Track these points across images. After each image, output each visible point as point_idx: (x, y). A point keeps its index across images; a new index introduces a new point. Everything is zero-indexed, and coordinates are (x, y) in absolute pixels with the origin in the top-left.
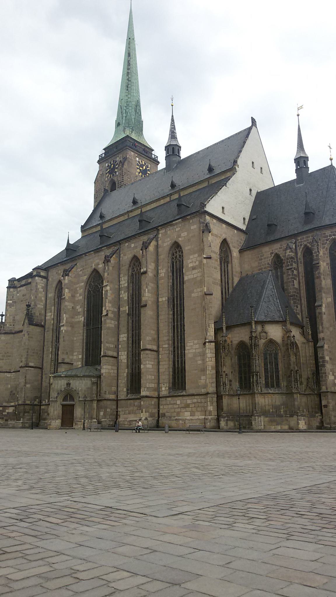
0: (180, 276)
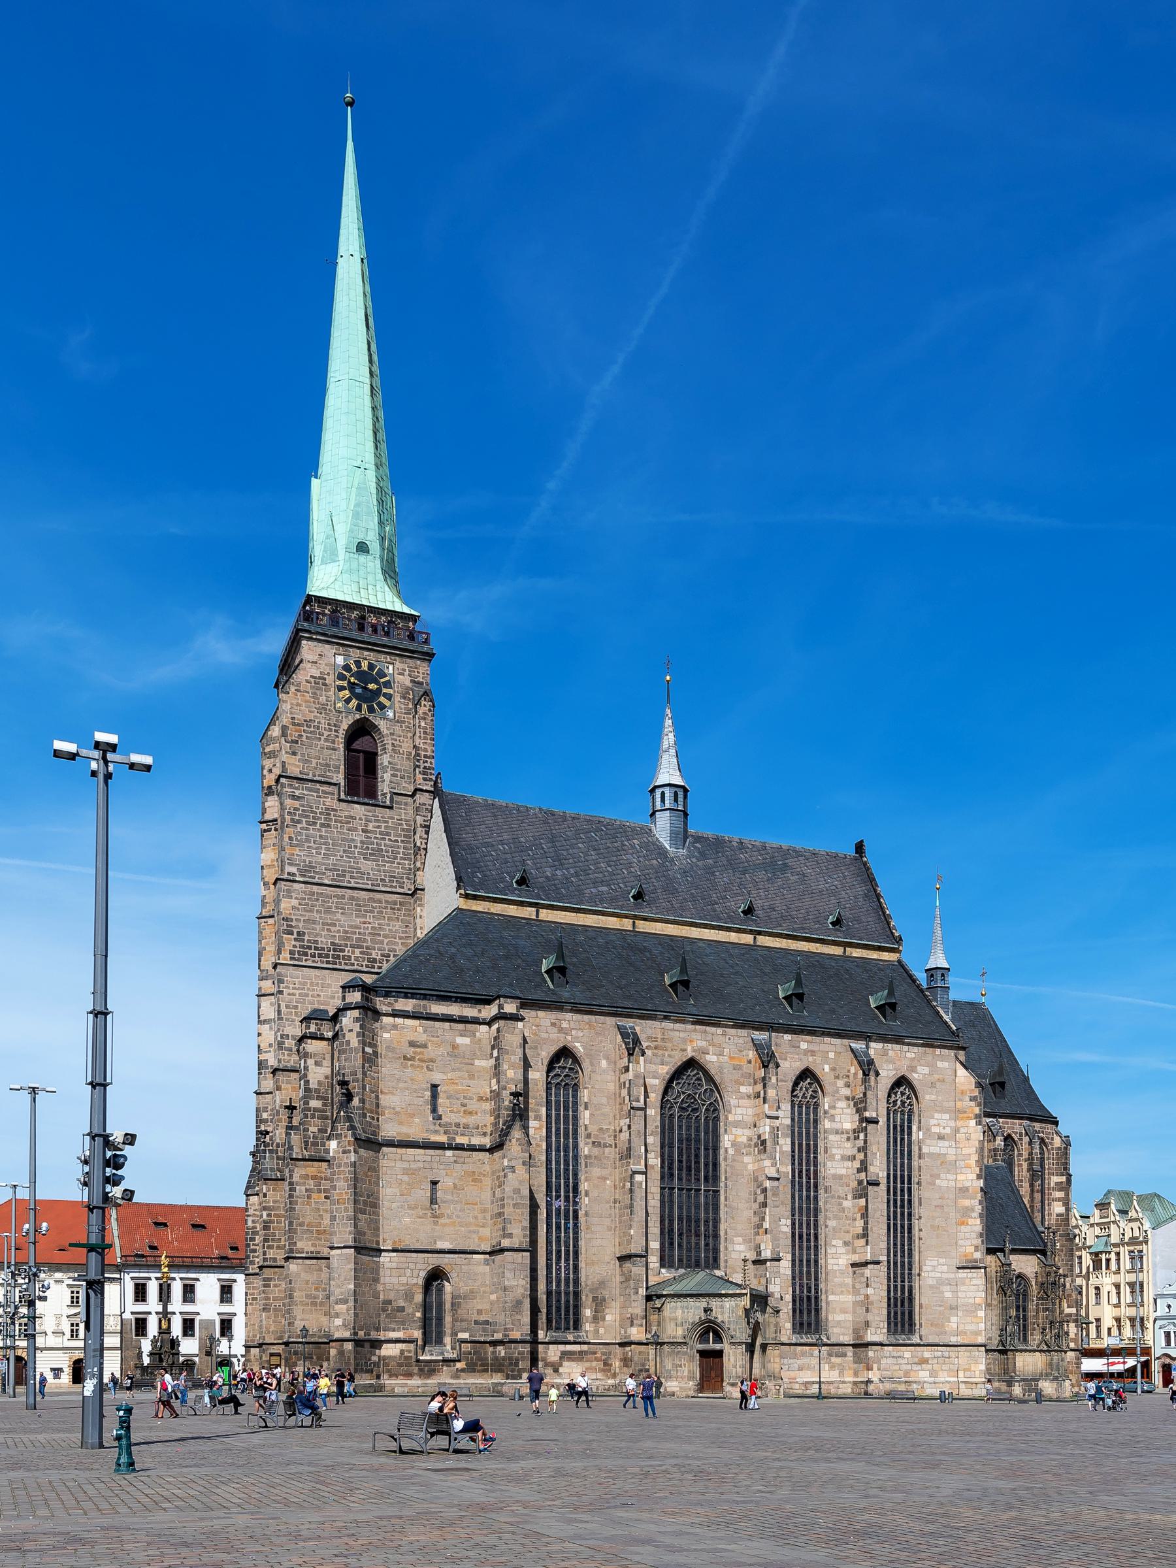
0: (902, 1139)
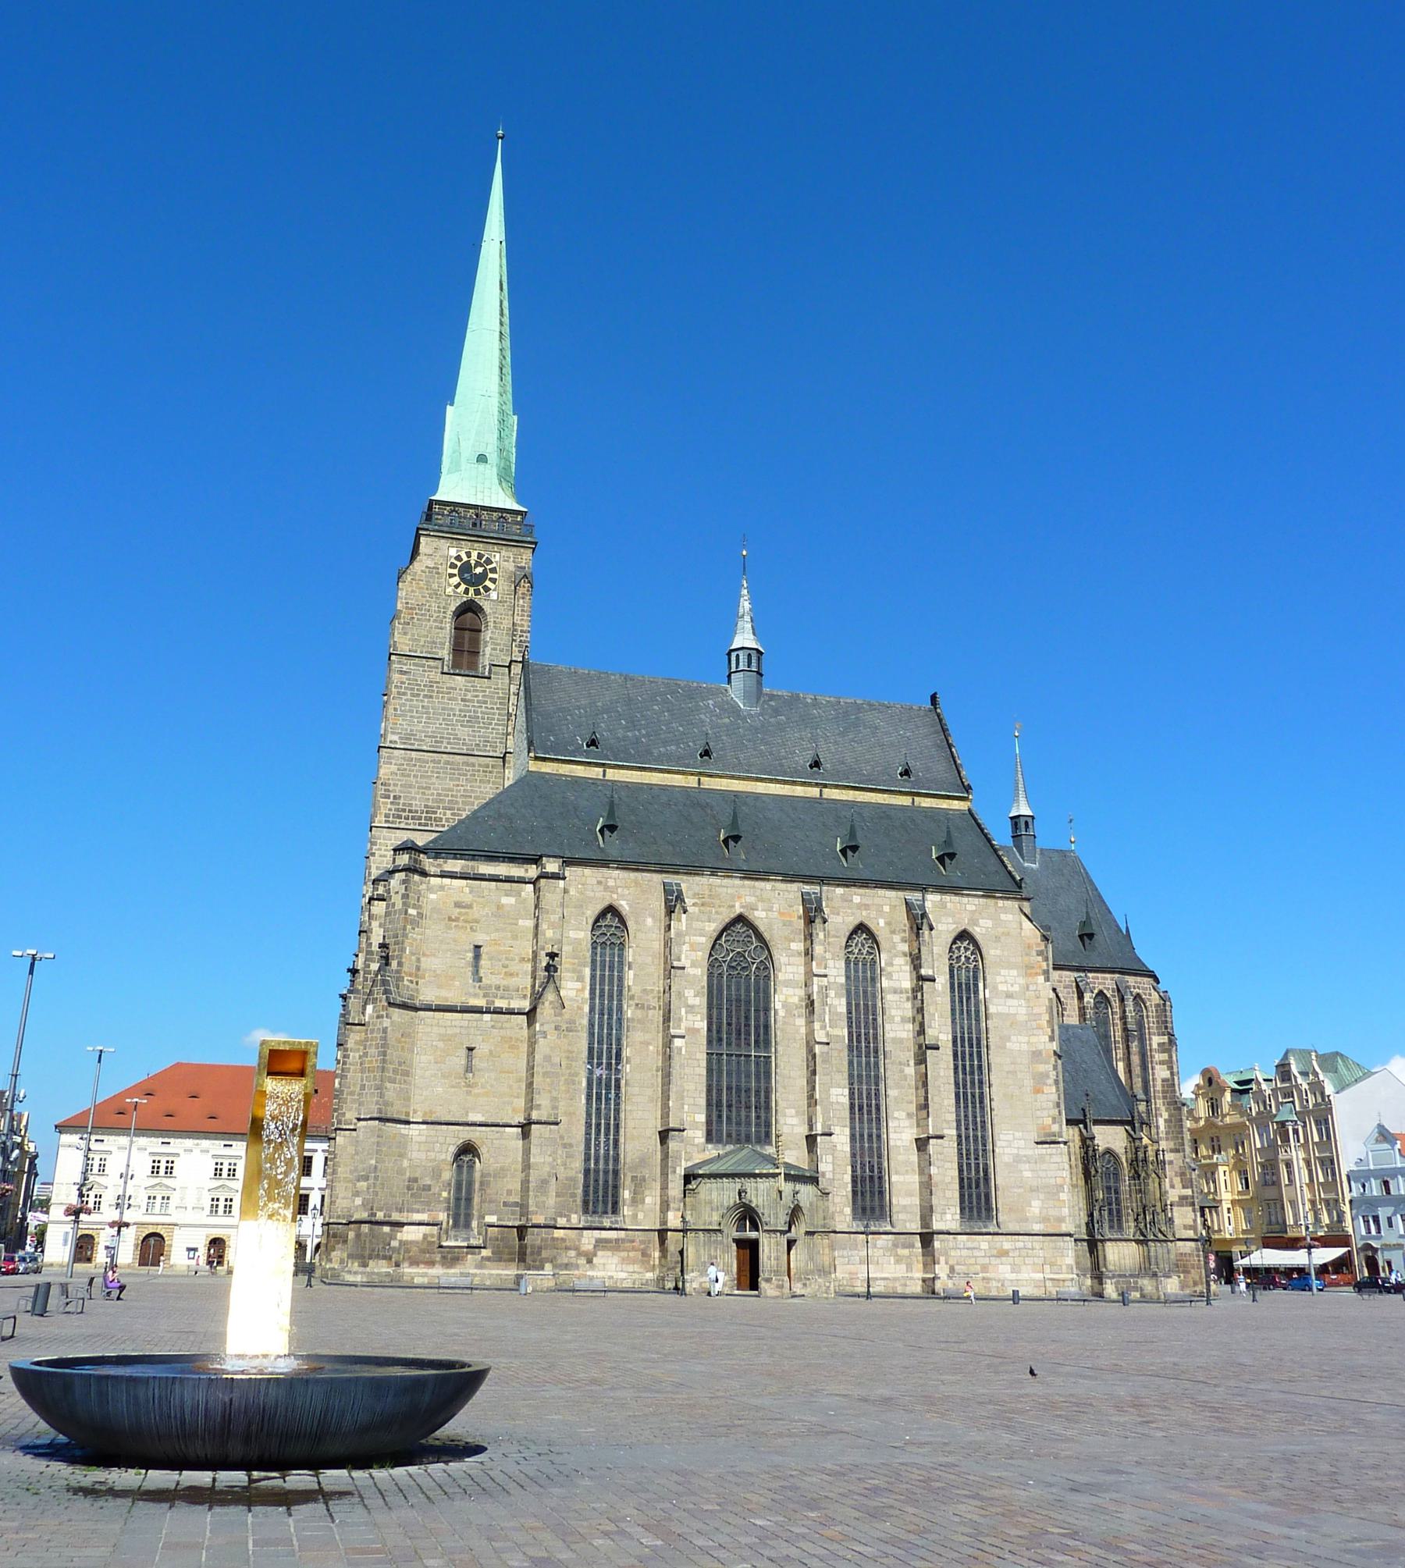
0: (968, 999)
